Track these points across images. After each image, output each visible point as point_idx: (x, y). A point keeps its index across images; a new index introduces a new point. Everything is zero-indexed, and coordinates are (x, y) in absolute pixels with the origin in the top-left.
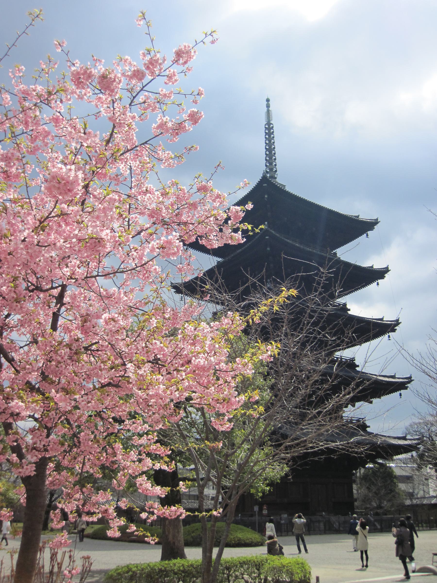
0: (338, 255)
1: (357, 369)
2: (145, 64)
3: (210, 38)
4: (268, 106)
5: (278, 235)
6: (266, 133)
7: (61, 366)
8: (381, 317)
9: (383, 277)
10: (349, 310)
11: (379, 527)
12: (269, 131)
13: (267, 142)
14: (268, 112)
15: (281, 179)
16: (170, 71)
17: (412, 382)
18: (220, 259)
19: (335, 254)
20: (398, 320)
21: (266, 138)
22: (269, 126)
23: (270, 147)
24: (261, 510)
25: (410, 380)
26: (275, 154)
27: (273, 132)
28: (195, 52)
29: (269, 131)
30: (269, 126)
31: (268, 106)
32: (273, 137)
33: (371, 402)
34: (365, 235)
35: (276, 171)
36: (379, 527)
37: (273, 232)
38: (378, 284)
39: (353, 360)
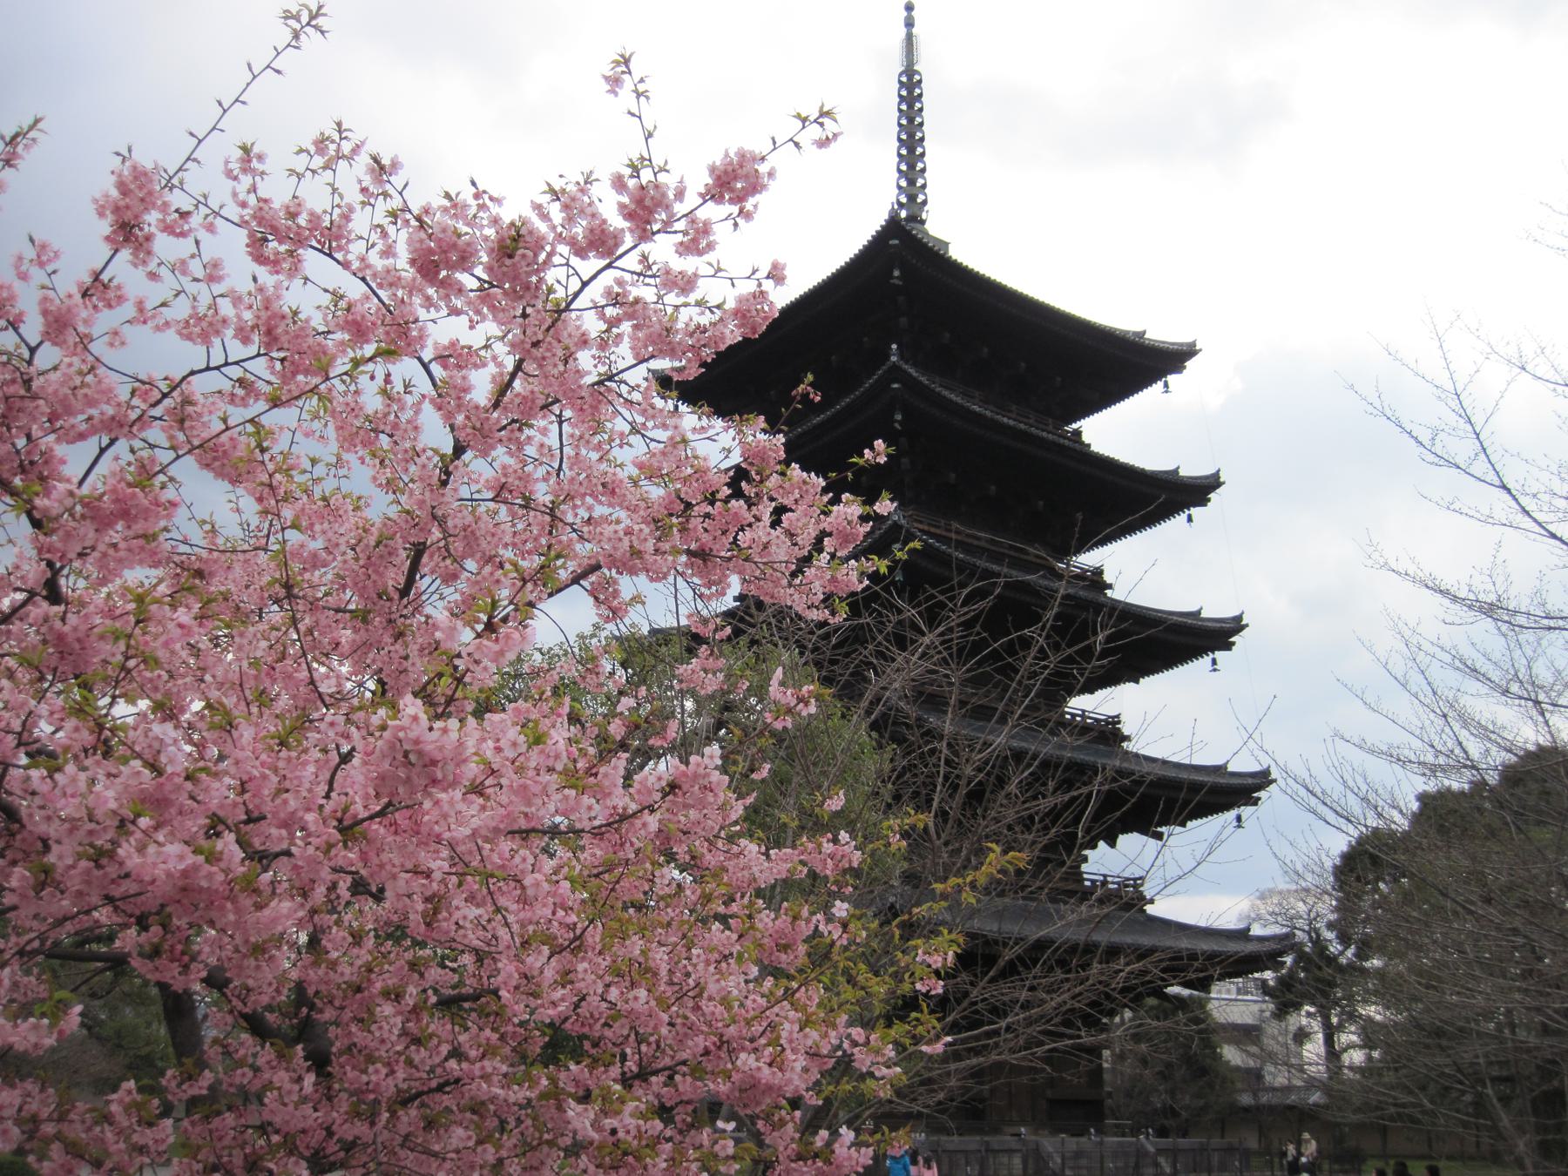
0: (1086, 438)
1: (1125, 745)
2: (622, 206)
3: (814, 132)
4: (909, 24)
5: (923, 379)
6: (900, 96)
7: (377, 1071)
8: (1193, 609)
9: (1202, 500)
11: (1168, 1170)
12: (910, 92)
13: (904, 122)
14: (909, 40)
15: (938, 224)
16: (693, 221)
17: (1272, 787)
19: (1078, 433)
20: (1239, 618)
21: (900, 111)
22: (910, 78)
23: (911, 136)
25: (1262, 779)
26: (923, 154)
27: (920, 95)
28: (771, 174)
29: (910, 92)
30: (910, 78)
31: (909, 24)
32: (921, 110)
33: (1159, 836)
34: (1160, 384)
35: (925, 203)
36: (1168, 1170)
37: (912, 371)
38: (1190, 519)
39: (1115, 721)
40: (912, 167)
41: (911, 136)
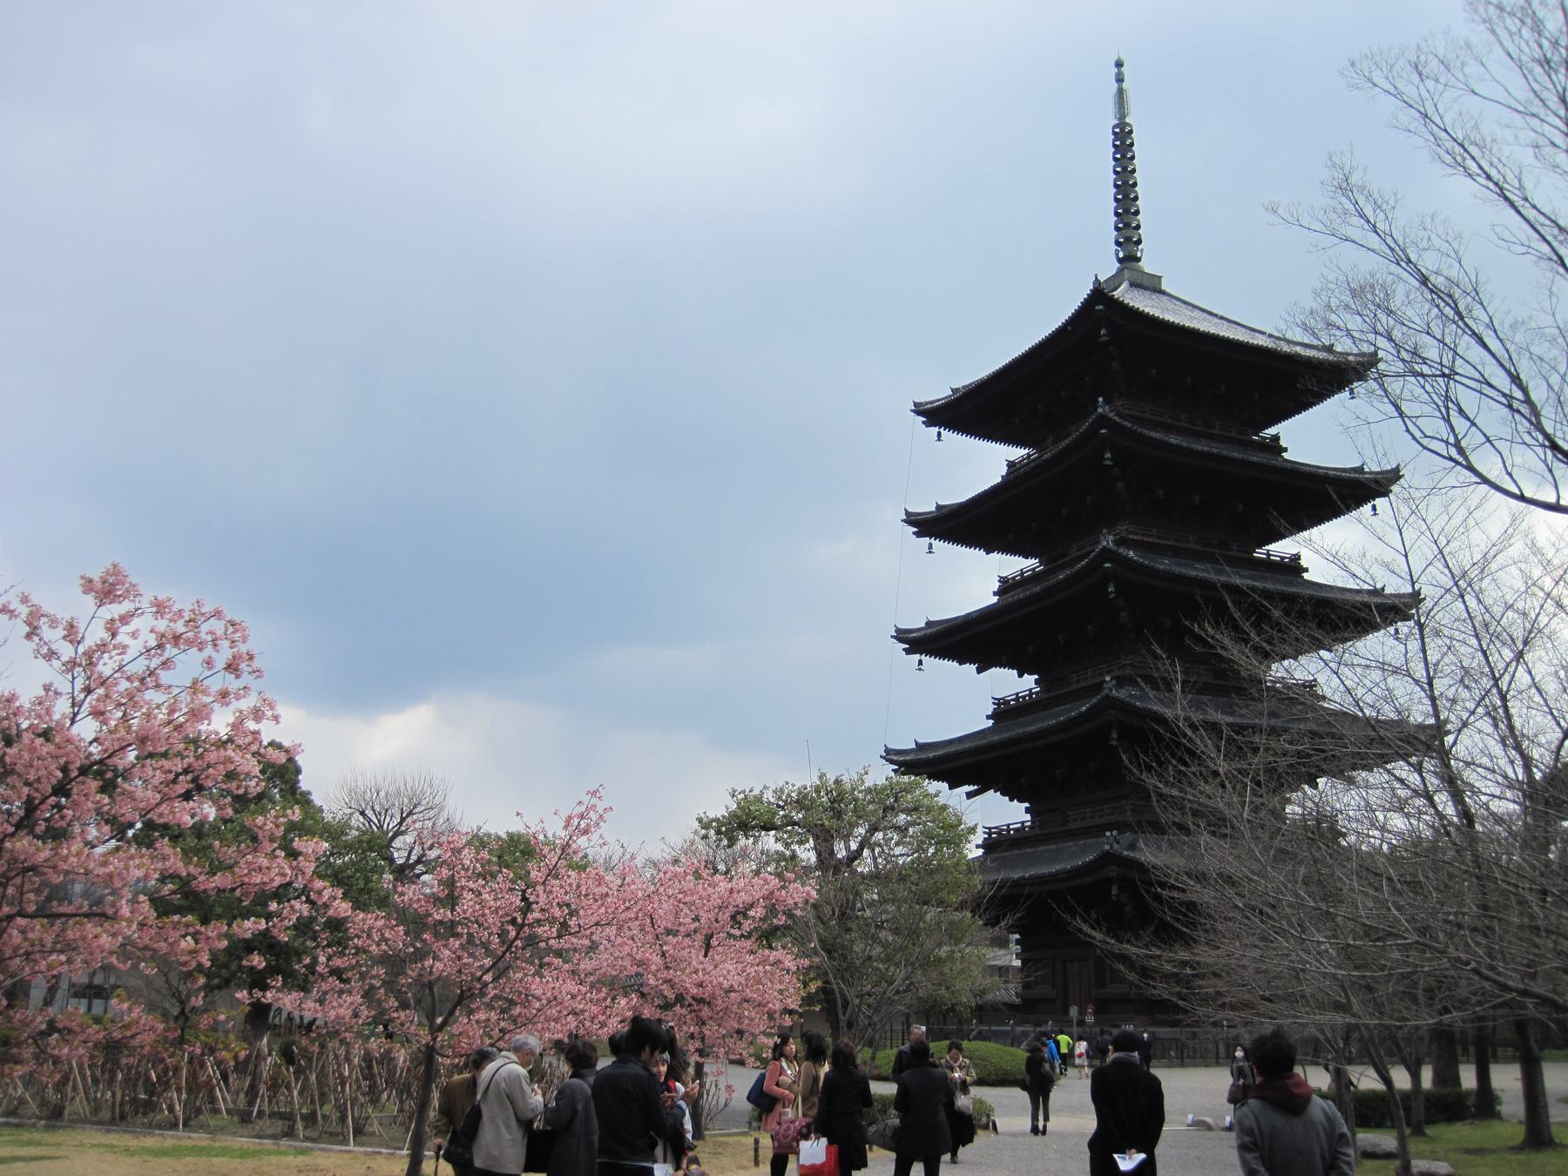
0: (1283, 443)
4: (1120, 79)
9: (1385, 493)
10: (1306, 570)
12: (1123, 143)
14: (1120, 93)
18: (1017, 453)
19: (1276, 438)
22: (1122, 130)
23: (1125, 183)
24: (1082, 1013)
27: (1132, 144)
29: (1123, 143)
30: (1122, 130)
31: (1120, 79)
33: (1351, 781)
34: (1346, 394)
35: (1139, 242)
38: (1374, 508)
40: (1127, 211)
41: (1125, 183)
